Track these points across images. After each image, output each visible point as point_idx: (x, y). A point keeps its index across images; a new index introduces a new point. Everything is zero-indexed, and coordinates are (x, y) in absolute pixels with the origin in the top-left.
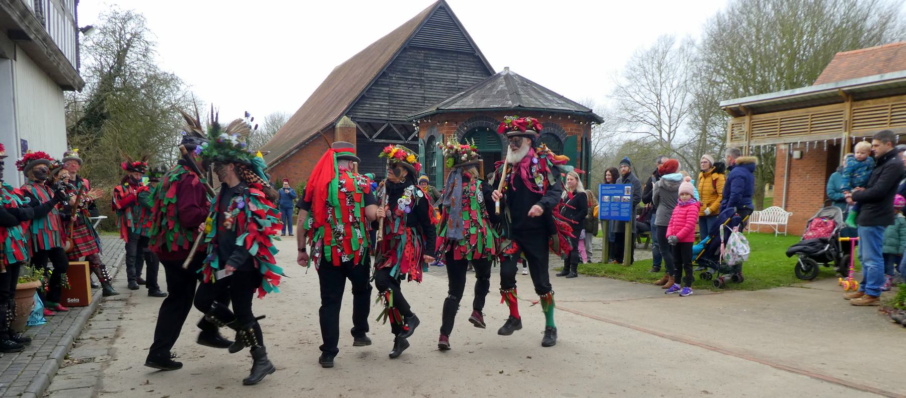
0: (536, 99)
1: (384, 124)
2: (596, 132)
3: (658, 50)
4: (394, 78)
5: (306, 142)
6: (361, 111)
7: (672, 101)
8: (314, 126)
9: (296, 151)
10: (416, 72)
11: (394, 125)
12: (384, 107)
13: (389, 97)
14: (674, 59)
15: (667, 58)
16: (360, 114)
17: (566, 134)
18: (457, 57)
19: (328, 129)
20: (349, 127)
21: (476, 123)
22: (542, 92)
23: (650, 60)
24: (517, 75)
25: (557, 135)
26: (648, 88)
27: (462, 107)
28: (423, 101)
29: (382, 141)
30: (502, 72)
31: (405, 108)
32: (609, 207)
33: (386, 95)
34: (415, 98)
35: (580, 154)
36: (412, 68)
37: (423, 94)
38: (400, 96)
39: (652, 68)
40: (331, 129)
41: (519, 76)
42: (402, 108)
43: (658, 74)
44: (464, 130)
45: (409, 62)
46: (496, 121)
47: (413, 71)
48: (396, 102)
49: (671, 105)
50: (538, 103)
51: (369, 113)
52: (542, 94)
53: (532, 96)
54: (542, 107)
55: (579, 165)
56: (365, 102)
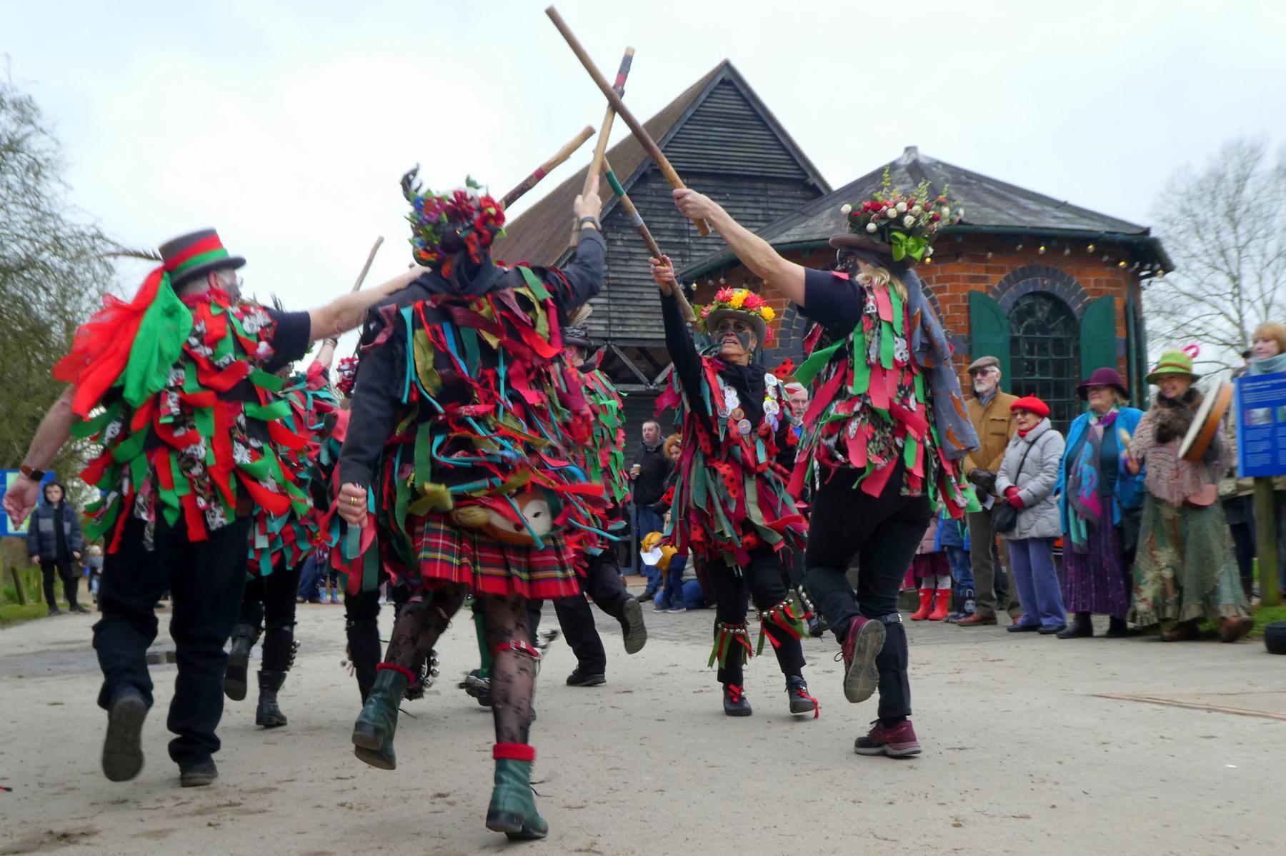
0: (999, 210)
2: (1155, 291)
3: (1224, 175)
4: (619, 243)
7: (1268, 287)
10: (671, 226)
11: (622, 349)
14: (1265, 193)
15: (1248, 192)
17: (1085, 294)
18: (766, 190)
22: (1009, 196)
23: (1208, 198)
24: (938, 162)
25: (1062, 297)
26: (1207, 260)
27: (806, 237)
30: (899, 159)
32: (1273, 438)
35: (1123, 344)
36: (660, 219)
38: (633, 283)
39: (1213, 216)
41: (946, 166)
42: (639, 309)
43: (1229, 228)
45: (654, 206)
47: (662, 226)
48: (626, 295)
49: (1268, 297)
52: (1009, 200)
53: (987, 205)
55: (1125, 371)
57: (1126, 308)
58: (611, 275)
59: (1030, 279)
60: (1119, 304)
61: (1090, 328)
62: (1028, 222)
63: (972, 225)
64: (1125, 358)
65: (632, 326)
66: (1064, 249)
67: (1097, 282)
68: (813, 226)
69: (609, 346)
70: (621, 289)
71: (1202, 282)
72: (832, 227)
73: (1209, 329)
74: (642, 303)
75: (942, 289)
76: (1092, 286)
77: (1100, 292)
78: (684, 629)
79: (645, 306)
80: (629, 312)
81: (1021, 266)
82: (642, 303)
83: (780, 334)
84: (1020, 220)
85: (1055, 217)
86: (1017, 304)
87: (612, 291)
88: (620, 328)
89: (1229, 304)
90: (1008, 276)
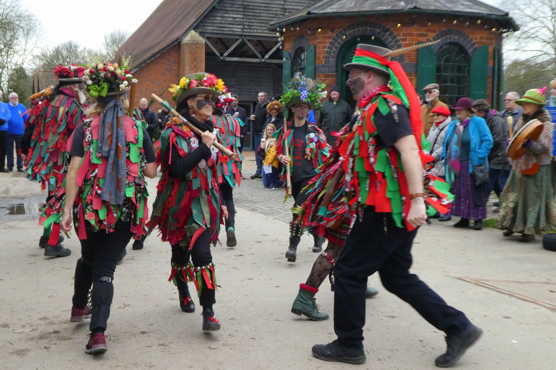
1: (237, 40)
5: (147, 60)
6: (211, 25)
8: (157, 42)
9: (135, 70)
11: (249, 40)
12: (237, 20)
13: (244, 8)
16: (209, 29)
17: (474, 44)
19: (172, 45)
20: (197, 44)
21: (358, 30)
27: (340, 10)
28: (282, 13)
29: (235, 59)
31: (261, 21)
33: (240, 6)
34: (274, 9)
37: (284, 5)
38: (256, 8)
40: (177, 45)
42: (258, 21)
44: (342, 40)
46: (384, 27)
50: (438, 4)
51: (220, 27)
54: (444, 9)
56: (216, 14)
57: (494, 50)
58: (245, 3)
59: (448, 36)
60: (491, 49)
61: (476, 61)
62: (449, 8)
63: (421, 9)
64: (492, 76)
65: (254, 29)
66: (466, 22)
67: (481, 38)
68: (344, 4)
69: (243, 39)
70: (250, 11)
71: (537, 10)
72: (353, 5)
73: (538, 34)
74: (260, 18)
75: (405, 40)
76: (478, 40)
77: (482, 43)
78: (271, 205)
79: (261, 20)
80: (253, 22)
81: (444, 29)
82: (260, 18)
83: (324, 57)
84: (446, 7)
85: (463, 5)
86: (441, 47)
87: (246, 12)
88: (249, 30)
89: (549, 22)
90: (437, 34)
